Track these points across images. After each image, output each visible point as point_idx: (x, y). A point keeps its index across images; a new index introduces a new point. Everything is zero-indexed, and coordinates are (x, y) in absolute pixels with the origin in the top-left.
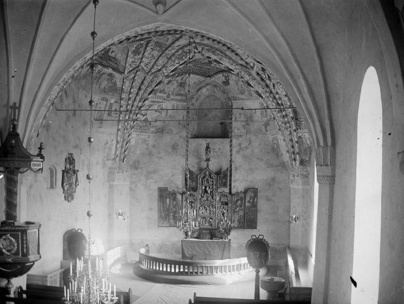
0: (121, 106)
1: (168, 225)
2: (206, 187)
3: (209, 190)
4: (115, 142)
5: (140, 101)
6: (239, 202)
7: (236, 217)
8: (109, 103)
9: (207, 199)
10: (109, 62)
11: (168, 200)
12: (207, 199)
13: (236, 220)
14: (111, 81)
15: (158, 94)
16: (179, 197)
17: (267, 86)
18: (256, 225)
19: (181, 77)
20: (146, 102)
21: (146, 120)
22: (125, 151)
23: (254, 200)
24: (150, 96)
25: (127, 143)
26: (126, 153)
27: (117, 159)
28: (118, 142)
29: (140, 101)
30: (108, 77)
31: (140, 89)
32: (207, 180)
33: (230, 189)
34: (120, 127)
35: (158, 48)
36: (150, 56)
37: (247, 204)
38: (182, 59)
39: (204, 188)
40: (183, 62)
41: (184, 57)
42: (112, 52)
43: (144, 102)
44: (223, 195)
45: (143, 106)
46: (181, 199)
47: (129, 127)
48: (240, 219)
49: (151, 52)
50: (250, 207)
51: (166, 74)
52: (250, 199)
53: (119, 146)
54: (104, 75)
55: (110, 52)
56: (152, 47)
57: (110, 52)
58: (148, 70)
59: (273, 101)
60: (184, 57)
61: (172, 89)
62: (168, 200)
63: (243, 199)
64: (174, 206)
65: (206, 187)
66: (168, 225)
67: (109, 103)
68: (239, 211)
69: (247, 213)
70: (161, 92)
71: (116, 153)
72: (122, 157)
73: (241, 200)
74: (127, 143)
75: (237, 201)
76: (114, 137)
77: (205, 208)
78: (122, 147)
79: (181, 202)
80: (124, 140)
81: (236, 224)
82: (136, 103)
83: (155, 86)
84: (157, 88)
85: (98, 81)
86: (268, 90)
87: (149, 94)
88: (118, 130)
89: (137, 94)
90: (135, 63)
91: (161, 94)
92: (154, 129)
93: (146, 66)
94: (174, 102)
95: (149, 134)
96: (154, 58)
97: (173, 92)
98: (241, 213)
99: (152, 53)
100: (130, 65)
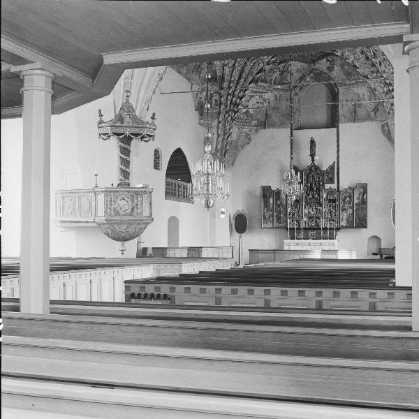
0: (221, 97)
1: (271, 226)
2: (311, 184)
4: (216, 136)
5: (241, 91)
6: (348, 199)
7: (344, 216)
8: (209, 94)
11: (271, 199)
15: (259, 84)
17: (373, 65)
18: (366, 222)
19: (283, 64)
20: (247, 92)
21: (247, 112)
22: (226, 145)
23: (364, 196)
24: (251, 85)
25: (228, 137)
26: (227, 148)
27: (218, 155)
28: (219, 136)
29: (241, 91)
31: (240, 77)
32: (313, 177)
33: (338, 187)
34: (220, 119)
37: (356, 201)
43: (245, 92)
44: (330, 192)
45: (244, 96)
47: (229, 119)
51: (267, 60)
53: (220, 139)
59: (381, 82)
61: (274, 78)
62: (271, 199)
64: (279, 206)
65: (311, 184)
67: (209, 94)
70: (262, 81)
71: (216, 147)
72: (223, 152)
74: (228, 137)
75: (345, 198)
76: (214, 131)
77: (310, 206)
78: (223, 140)
80: (225, 134)
81: (343, 223)
82: (236, 93)
83: (256, 74)
84: (258, 75)
85: (198, 69)
86: (374, 69)
87: (250, 83)
88: (219, 122)
89: (238, 83)
91: (262, 84)
94: (276, 93)
97: (275, 81)
98: (350, 211)
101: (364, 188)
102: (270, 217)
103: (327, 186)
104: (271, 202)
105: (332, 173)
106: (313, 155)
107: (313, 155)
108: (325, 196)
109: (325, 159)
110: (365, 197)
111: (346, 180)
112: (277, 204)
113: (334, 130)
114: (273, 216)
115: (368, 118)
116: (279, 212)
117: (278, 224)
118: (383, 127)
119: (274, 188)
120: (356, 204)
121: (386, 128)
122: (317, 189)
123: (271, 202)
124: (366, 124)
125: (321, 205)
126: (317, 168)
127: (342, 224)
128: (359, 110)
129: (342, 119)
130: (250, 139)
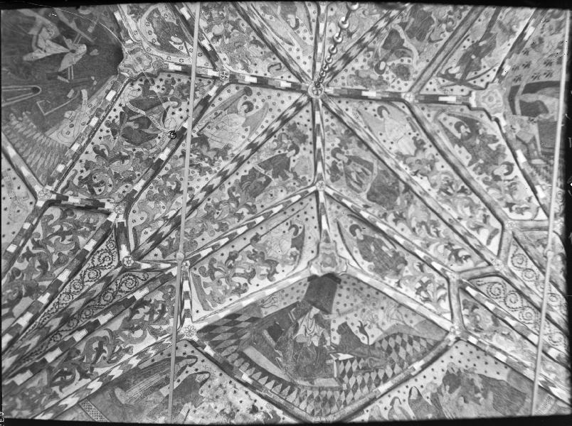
10: (393, 355)
14: (477, 391)
30: (456, 394)
35: (398, 201)
36: (423, 233)
38: (499, 152)
40: (508, 151)
41: (493, 146)
42: (362, 329)
49: (409, 226)
54: (443, 400)
55: (360, 336)
56: (391, 217)
57: (360, 336)
58: (477, 257)
60: (493, 146)
90: (430, 287)
93: (459, 259)
96: (435, 224)
99: (414, 224)
100: (427, 300)
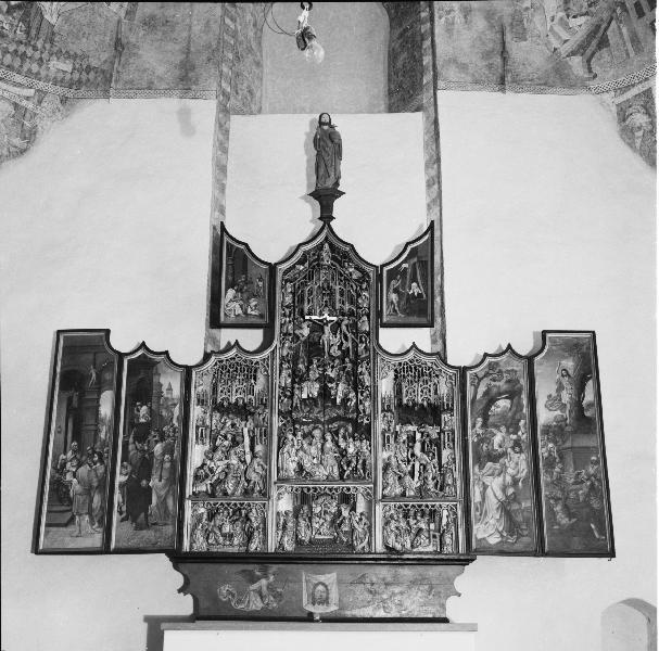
3: (336, 340)
6: (503, 404)
7: (491, 487)
9: (325, 393)
12: (325, 393)
13: (492, 502)
16: (171, 384)
23: (581, 390)
37: (545, 416)
39: (306, 332)
44: (411, 370)
46: (177, 392)
48: (515, 498)
50: (557, 431)
52: (560, 388)
63: (522, 390)
66: (96, 540)
68: (504, 454)
69: (550, 464)
73: (512, 394)
75: (491, 400)
79: (177, 411)
81: (488, 529)
92: (67, 66)
95: (41, 85)
98: (518, 464)
101: (582, 354)
102: (88, 491)
103: (393, 340)
104: (106, 410)
105: (416, 283)
106: (325, 196)
107: (325, 196)
108: (386, 387)
109: (375, 230)
110: (589, 396)
111: (480, 320)
112: (132, 423)
113: (413, 122)
114: (106, 485)
115: (556, 78)
116: (144, 467)
117: (128, 527)
118: (623, 115)
119: (122, 342)
120: (547, 429)
121: (640, 119)
122: (345, 353)
123: (106, 410)
124: (552, 101)
125: (364, 432)
126: (344, 254)
127: (479, 531)
128: (517, 50)
129: (450, 73)
130: (30, 136)
